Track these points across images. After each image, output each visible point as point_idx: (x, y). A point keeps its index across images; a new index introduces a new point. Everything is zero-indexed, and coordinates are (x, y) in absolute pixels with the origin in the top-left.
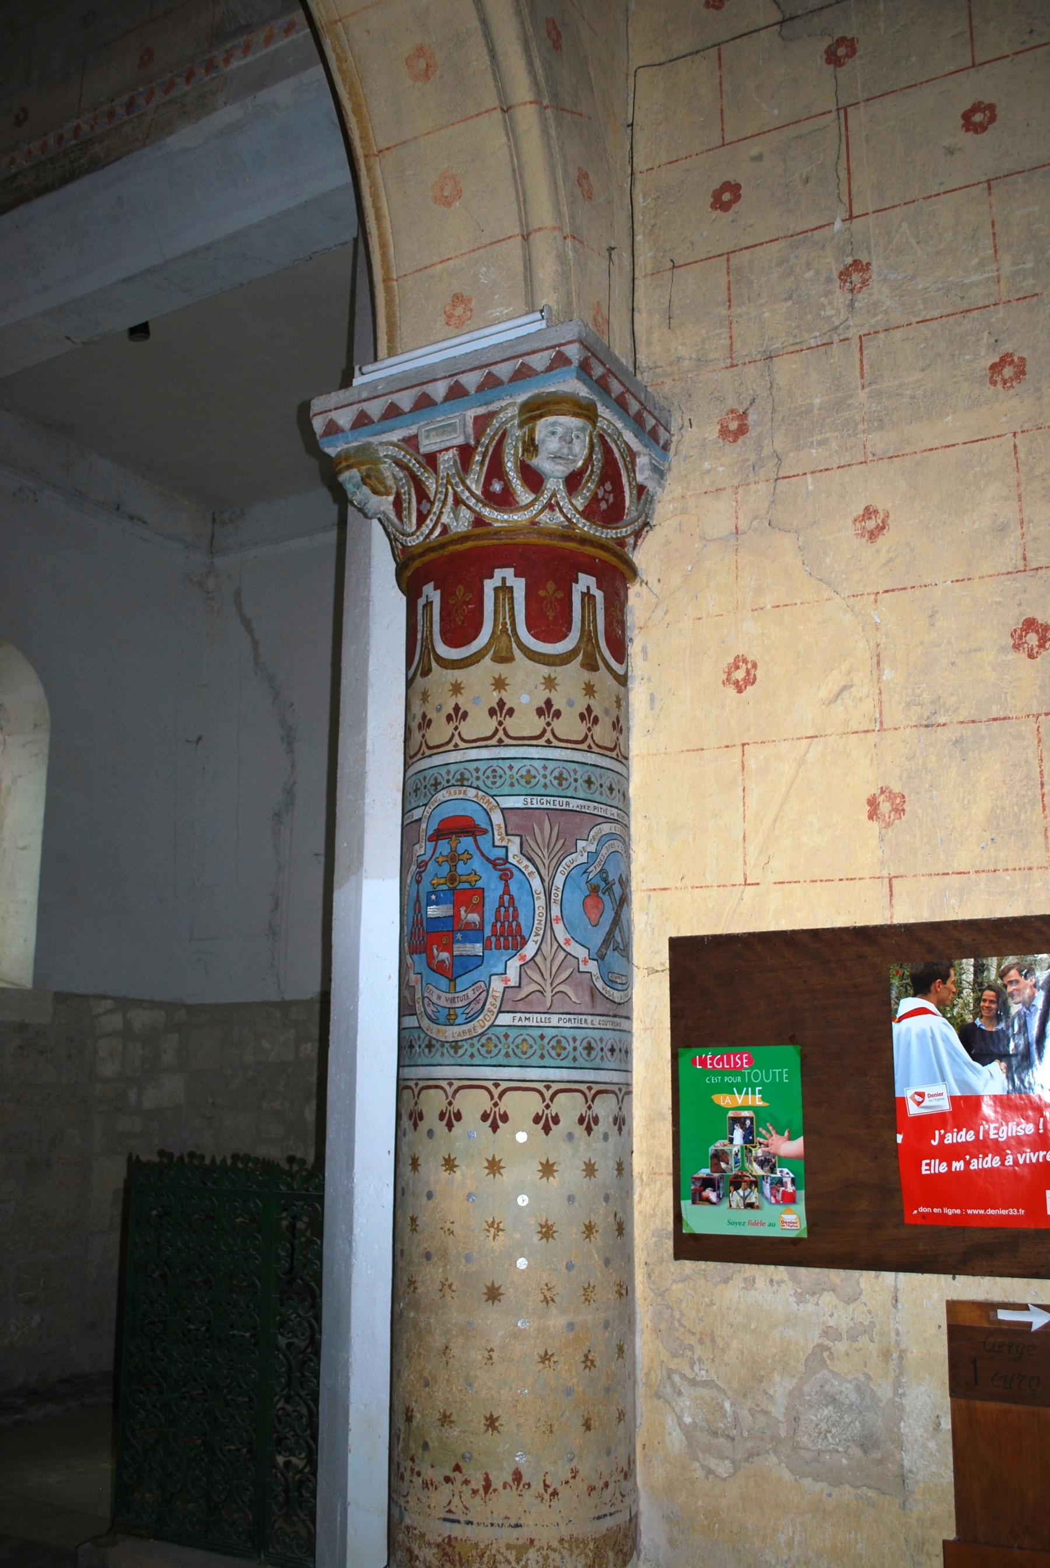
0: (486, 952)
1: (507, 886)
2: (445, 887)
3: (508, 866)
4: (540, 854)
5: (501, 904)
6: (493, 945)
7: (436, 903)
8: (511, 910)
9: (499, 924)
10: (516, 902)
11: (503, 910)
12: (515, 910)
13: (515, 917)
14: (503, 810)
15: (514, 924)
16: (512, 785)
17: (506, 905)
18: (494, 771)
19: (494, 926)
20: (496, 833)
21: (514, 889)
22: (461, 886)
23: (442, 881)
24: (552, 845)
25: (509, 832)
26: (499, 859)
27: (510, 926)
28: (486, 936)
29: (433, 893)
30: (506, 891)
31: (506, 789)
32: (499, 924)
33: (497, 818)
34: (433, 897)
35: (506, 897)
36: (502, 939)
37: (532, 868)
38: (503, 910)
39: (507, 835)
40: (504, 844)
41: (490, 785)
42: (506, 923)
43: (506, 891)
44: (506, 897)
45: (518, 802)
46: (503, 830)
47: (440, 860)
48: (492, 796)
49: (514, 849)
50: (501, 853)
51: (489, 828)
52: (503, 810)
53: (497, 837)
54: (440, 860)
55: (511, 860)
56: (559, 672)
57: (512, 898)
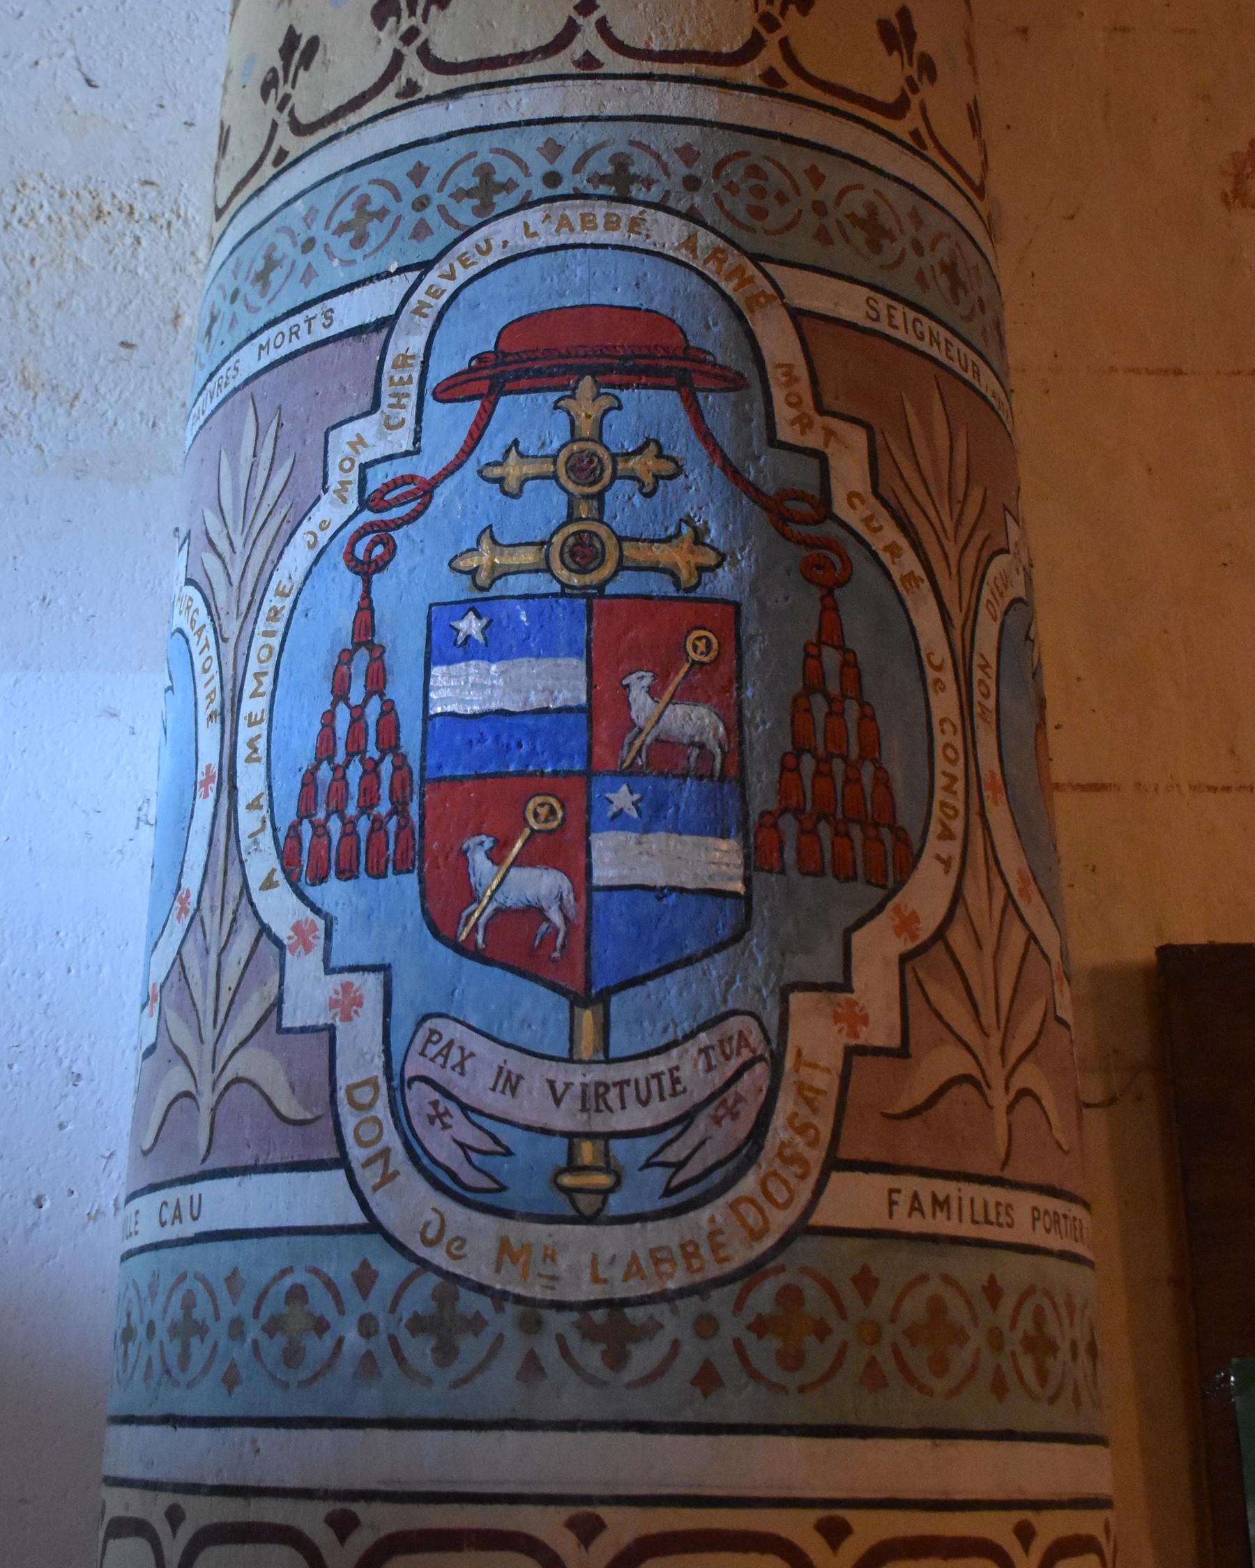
0: (759, 879)
1: (829, 608)
2: (543, 584)
3: (830, 529)
4: (932, 514)
5: (813, 684)
6: (790, 856)
7: (491, 648)
8: (852, 709)
9: (808, 764)
10: (866, 681)
11: (819, 705)
12: (867, 716)
13: (871, 747)
14: (797, 316)
15: (868, 771)
16: (823, 236)
17: (833, 687)
18: (754, 171)
19: (789, 767)
20: (778, 395)
21: (857, 629)
22: (625, 584)
23: (527, 557)
24: (959, 493)
25: (828, 401)
26: (799, 496)
27: (852, 780)
28: (756, 806)
29: (471, 607)
30: (830, 630)
31: (801, 245)
32: (808, 764)
33: (778, 341)
34: (471, 626)
35: (831, 657)
36: (824, 830)
37: (910, 562)
38: (819, 705)
39: (821, 410)
40: (813, 440)
41: (743, 216)
42: (838, 766)
43: (830, 630)
44: (831, 657)
45: (849, 303)
46: (804, 387)
47: (513, 470)
48: (756, 259)
49: (849, 473)
50: (804, 475)
51: (750, 372)
52: (797, 316)
53: (783, 413)
54: (513, 470)
55: (840, 507)
57: (850, 663)
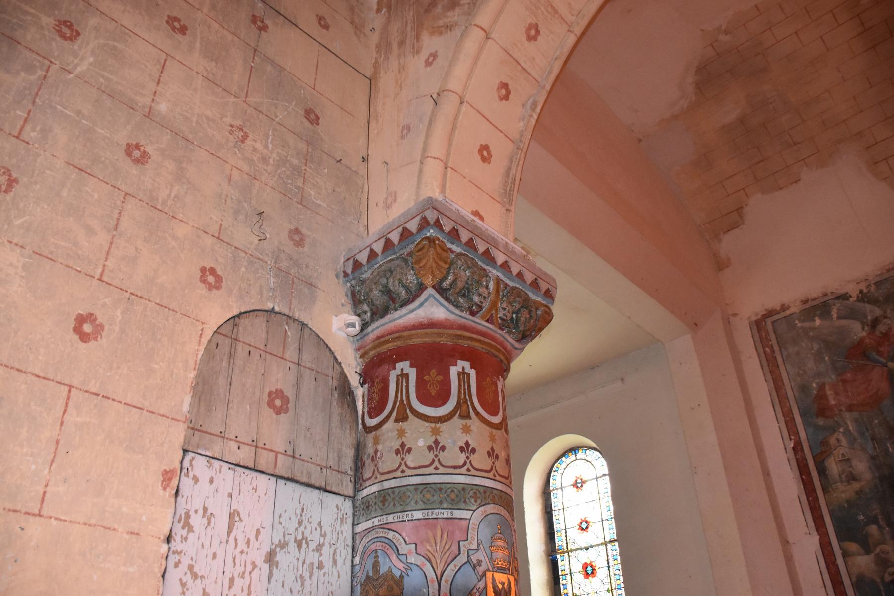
56: (444, 427)
